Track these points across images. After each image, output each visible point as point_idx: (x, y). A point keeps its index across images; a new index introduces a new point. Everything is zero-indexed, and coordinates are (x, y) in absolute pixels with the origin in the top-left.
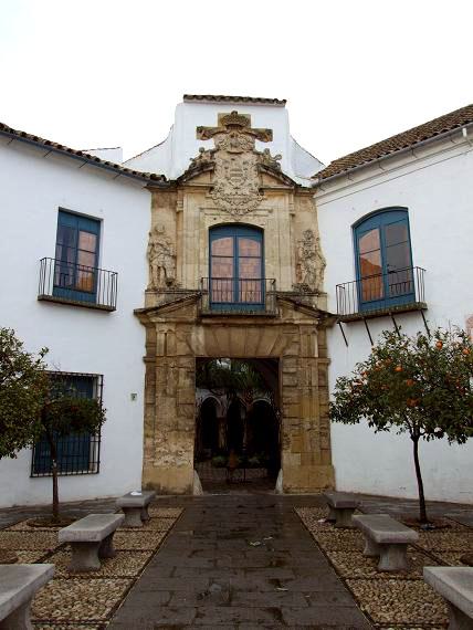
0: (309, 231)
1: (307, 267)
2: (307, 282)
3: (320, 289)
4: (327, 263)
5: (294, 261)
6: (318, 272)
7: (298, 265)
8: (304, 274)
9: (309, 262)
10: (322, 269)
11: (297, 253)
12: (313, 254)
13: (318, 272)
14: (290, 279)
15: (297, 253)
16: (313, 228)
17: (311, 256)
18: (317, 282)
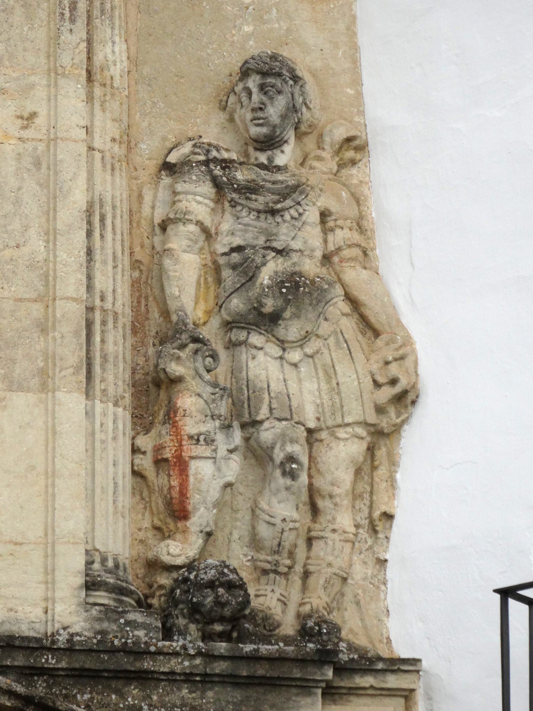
0: (270, 72)
1: (242, 412)
2: (238, 557)
3: (353, 630)
4: (431, 371)
5: (116, 343)
6: (341, 455)
7: (152, 395)
8: (211, 473)
9: (263, 363)
10: (381, 437)
11: (148, 279)
12: (295, 289)
13: (341, 455)
14: (72, 521)
15: (148, 279)
16: (308, 50)
17: (270, 304)
18: (330, 554)
